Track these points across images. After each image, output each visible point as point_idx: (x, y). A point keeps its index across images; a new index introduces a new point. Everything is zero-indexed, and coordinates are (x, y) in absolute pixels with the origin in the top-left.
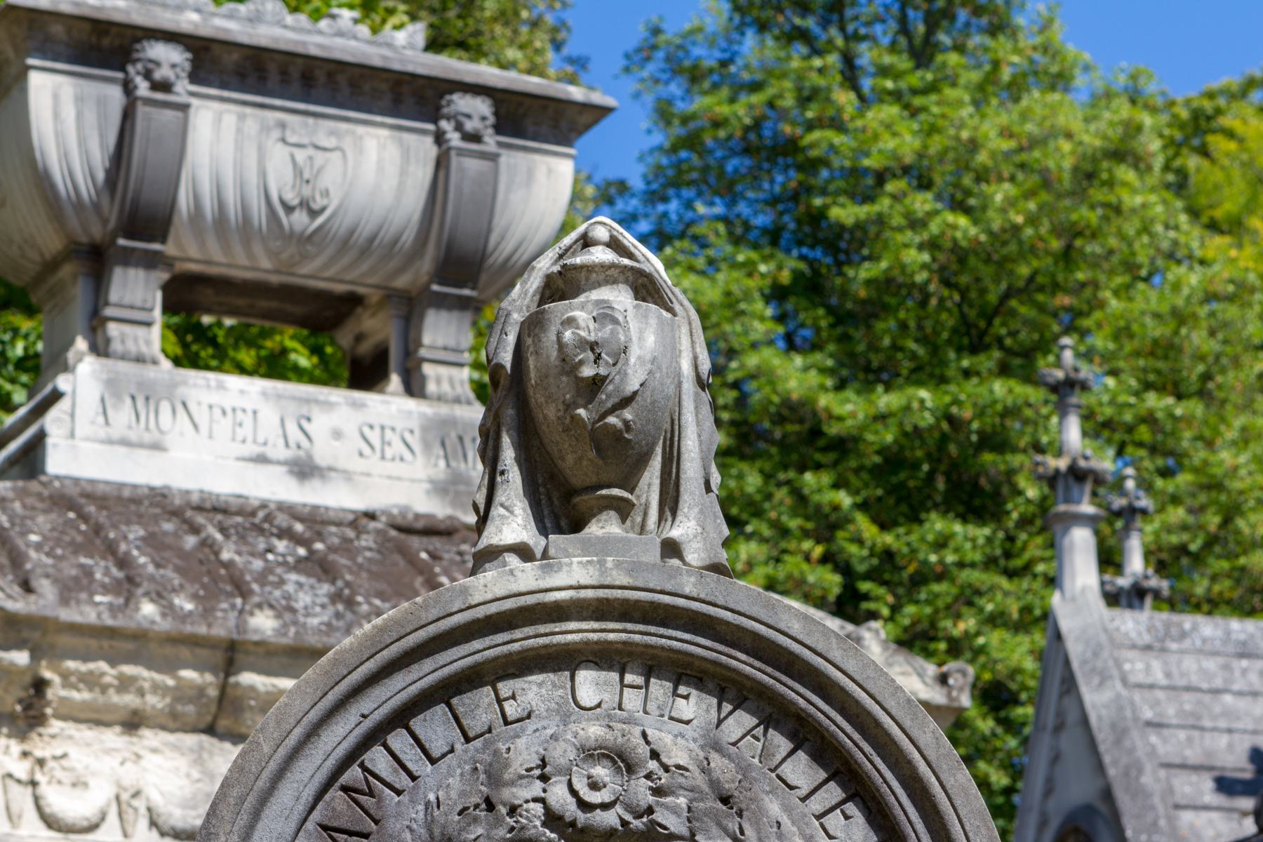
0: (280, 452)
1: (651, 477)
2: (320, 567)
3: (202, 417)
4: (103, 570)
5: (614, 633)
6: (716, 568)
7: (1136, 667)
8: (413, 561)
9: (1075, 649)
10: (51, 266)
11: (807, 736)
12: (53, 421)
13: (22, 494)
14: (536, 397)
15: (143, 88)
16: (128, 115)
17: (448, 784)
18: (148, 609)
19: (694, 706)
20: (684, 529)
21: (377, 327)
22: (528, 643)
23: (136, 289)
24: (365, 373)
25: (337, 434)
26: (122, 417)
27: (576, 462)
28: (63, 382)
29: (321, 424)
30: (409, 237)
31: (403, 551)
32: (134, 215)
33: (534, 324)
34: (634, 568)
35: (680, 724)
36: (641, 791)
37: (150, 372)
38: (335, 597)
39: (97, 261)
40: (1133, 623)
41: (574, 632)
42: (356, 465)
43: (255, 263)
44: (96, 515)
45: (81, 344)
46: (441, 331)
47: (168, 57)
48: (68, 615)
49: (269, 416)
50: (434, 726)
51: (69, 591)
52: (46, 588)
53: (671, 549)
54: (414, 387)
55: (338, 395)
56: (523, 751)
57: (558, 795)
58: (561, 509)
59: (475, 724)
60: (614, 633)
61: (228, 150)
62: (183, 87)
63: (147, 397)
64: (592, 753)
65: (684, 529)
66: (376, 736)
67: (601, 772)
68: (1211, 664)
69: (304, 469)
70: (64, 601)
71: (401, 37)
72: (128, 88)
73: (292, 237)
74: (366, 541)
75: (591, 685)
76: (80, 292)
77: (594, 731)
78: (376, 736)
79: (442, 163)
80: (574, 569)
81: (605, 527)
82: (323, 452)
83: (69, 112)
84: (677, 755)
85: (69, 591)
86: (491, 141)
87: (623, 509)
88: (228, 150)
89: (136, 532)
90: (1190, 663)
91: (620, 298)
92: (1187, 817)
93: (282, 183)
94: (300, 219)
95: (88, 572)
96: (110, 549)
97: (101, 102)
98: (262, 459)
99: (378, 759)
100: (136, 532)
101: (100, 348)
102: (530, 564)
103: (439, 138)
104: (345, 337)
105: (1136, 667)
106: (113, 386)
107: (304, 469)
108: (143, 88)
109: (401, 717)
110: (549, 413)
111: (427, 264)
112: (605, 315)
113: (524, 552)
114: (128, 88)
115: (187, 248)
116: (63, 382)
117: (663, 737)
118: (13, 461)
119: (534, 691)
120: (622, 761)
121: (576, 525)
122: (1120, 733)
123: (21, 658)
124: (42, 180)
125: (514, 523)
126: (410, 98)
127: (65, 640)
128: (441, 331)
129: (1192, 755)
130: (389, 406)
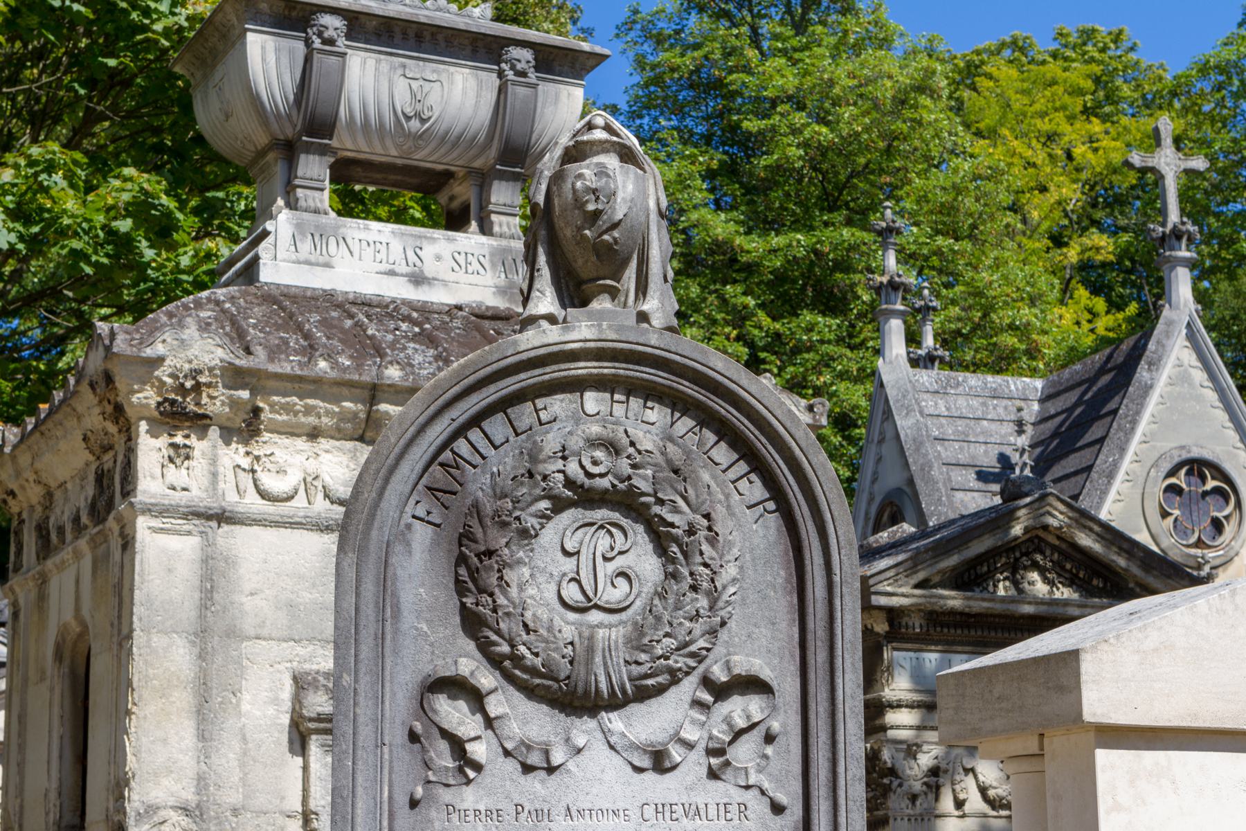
0: (403, 269)
1: (631, 273)
2: (429, 339)
3: (355, 247)
4: (294, 341)
5: (607, 369)
6: (670, 329)
7: (929, 404)
9: (891, 392)
10: (262, 153)
11: (726, 432)
12: (264, 249)
13: (244, 294)
14: (559, 223)
15: (317, 43)
16: (308, 60)
17: (505, 462)
18: (323, 364)
19: (657, 414)
20: (650, 305)
21: (463, 191)
22: (553, 375)
23: (314, 168)
24: (455, 220)
25: (438, 258)
26: (306, 246)
27: (584, 264)
28: (269, 225)
29: (428, 251)
30: (482, 136)
32: (312, 122)
33: (558, 178)
34: (620, 329)
35: (646, 425)
36: (624, 466)
37: (323, 219)
38: (437, 358)
39: (290, 150)
40: (926, 377)
41: (582, 368)
42: (451, 277)
43: (388, 152)
44: (290, 306)
45: (280, 202)
46: (502, 194)
47: (332, 23)
48: (273, 368)
49: (397, 246)
50: (497, 427)
52: (260, 352)
53: (643, 317)
54: (486, 229)
55: (438, 234)
56: (551, 441)
57: (573, 468)
58: (574, 292)
59: (521, 425)
60: (607, 369)
61: (370, 82)
62: (342, 42)
63: (321, 235)
64: (593, 443)
65: (650, 305)
66: (461, 432)
67: (599, 454)
68: (975, 403)
69: (418, 279)
70: (271, 359)
71: (477, 12)
73: (409, 135)
74: (457, 323)
75: (593, 401)
76: (279, 169)
77: (595, 429)
78: (461, 432)
79: (502, 90)
80: (583, 329)
81: (602, 304)
82: (430, 269)
84: (646, 444)
86: (532, 76)
87: (613, 293)
88: (370, 82)
89: (315, 317)
90: (961, 402)
91: (611, 161)
93: (403, 100)
94: (415, 125)
95: (286, 342)
96: (299, 328)
97: (291, 52)
98: (392, 273)
99: (462, 446)
100: (315, 317)
101: (292, 205)
102: (555, 326)
103: (501, 74)
104: (443, 198)
105: (929, 404)
106: (300, 227)
107: (418, 279)
108: (317, 43)
109: (476, 421)
110: (567, 233)
111: (493, 153)
112: (602, 172)
113: (552, 319)
114: (308, 43)
115: (345, 143)
116: (269, 225)
117: (638, 433)
118: (239, 274)
119: (558, 405)
120: (612, 447)
121: (584, 303)
122: (919, 444)
123: (245, 394)
124: (255, 99)
125: (545, 302)
126: (481, 49)
127: (271, 384)
128: (502, 194)
129: (963, 458)
130: (470, 241)
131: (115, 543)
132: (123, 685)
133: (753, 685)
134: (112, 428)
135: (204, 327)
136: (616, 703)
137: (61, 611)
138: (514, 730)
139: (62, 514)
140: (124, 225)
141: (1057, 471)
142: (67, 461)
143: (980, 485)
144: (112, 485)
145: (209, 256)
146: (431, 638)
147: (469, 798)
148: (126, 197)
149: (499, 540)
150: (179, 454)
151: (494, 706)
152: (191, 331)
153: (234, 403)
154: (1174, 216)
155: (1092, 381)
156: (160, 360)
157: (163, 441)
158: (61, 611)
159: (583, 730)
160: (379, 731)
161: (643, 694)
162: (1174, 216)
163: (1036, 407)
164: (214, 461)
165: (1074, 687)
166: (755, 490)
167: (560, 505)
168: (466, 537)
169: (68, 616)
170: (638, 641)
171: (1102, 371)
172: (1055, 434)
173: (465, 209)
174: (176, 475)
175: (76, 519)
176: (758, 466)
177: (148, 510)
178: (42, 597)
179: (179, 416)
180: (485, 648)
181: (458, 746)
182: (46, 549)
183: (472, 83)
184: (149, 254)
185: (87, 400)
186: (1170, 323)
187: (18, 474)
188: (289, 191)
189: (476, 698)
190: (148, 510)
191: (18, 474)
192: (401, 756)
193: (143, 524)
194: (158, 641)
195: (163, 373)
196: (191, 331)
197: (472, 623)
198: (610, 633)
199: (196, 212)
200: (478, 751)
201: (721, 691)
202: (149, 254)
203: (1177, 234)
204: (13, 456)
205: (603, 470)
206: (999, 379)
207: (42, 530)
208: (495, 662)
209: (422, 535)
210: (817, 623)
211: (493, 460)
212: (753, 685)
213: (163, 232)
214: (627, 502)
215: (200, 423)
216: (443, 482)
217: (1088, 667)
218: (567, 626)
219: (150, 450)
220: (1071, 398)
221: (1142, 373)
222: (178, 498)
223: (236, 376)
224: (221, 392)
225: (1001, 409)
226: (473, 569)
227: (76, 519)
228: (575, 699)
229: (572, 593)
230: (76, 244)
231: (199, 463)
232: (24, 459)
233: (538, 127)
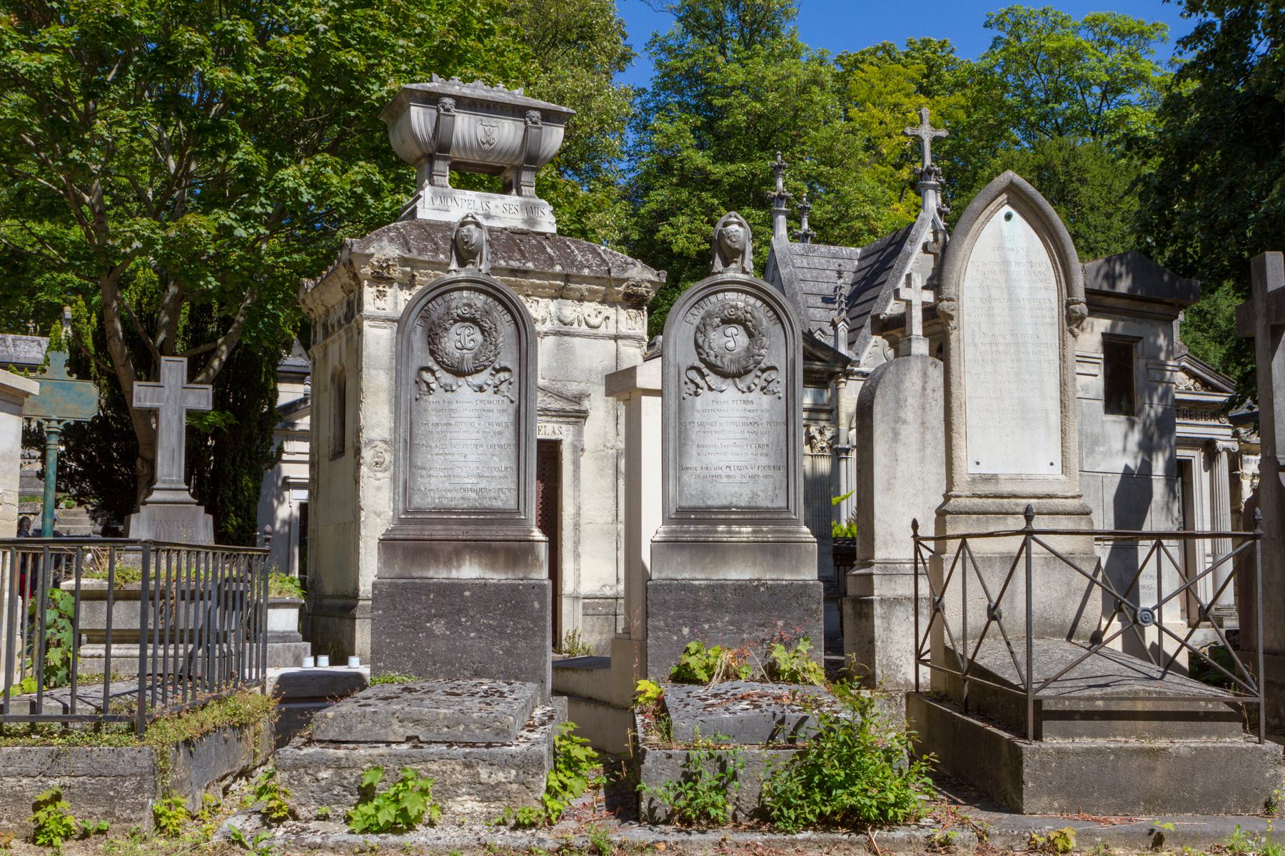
4: (430, 246)
5: (469, 285)
7: (798, 261)
8: (515, 242)
9: (778, 255)
10: (418, 159)
15: (442, 111)
16: (438, 118)
17: (441, 310)
18: (442, 256)
19: (482, 297)
21: (510, 175)
22: (454, 286)
23: (441, 166)
24: (506, 190)
26: (437, 202)
27: (465, 255)
28: (421, 193)
29: (492, 204)
30: (517, 151)
31: (512, 239)
32: (440, 146)
35: (480, 300)
37: (445, 190)
39: (431, 158)
40: (798, 247)
43: (475, 158)
44: (430, 229)
46: (526, 177)
47: (449, 102)
48: (420, 258)
49: (478, 202)
50: (439, 300)
51: (420, 252)
52: (414, 251)
54: (519, 193)
55: (497, 196)
56: (453, 305)
58: (462, 263)
60: (469, 285)
61: (466, 127)
62: (453, 109)
63: (444, 197)
66: (430, 302)
68: (823, 261)
71: (517, 92)
72: (438, 110)
73: (484, 151)
74: (504, 237)
75: (465, 293)
76: (426, 167)
78: (430, 302)
79: (526, 130)
80: (463, 274)
81: (470, 266)
83: (422, 118)
85: (420, 252)
86: (540, 124)
88: (466, 127)
89: (440, 235)
90: (816, 260)
91: (472, 227)
92: (811, 310)
93: (481, 136)
94: (487, 146)
96: (433, 240)
97: (431, 114)
100: (440, 235)
101: (432, 183)
102: (456, 272)
103: (526, 123)
104: (502, 178)
105: (798, 261)
106: (435, 194)
108: (442, 111)
109: (434, 299)
111: (522, 158)
112: (469, 230)
114: (438, 110)
115: (454, 154)
116: (421, 193)
119: (456, 294)
120: (470, 306)
122: (791, 283)
123: (408, 269)
124: (414, 136)
125: (454, 266)
126: (517, 111)
128: (526, 177)
129: (815, 290)
130: (512, 199)
131: (355, 331)
132: (359, 390)
133: (506, 369)
134: (353, 283)
135: (391, 240)
136: (470, 374)
137: (333, 361)
138: (443, 381)
139: (333, 319)
140: (359, 190)
141: (863, 298)
142: (335, 296)
143: (824, 305)
144: (354, 306)
145: (398, 202)
146: (421, 356)
147: (431, 398)
148: (360, 177)
149: (439, 331)
150: (381, 294)
152: (385, 242)
153: (404, 273)
154: (928, 162)
155: (884, 250)
156: (372, 255)
157: (374, 289)
158: (333, 361)
159: (461, 381)
160: (407, 379)
161: (477, 372)
162: (928, 162)
163: (856, 263)
164: (396, 297)
165: (634, 378)
166: (508, 317)
167: (456, 322)
168: (431, 330)
169: (336, 363)
170: (475, 358)
171: (889, 245)
172: (864, 278)
173: (511, 183)
174: (380, 303)
175: (339, 321)
176: (510, 311)
177: (368, 318)
178: (325, 355)
179: (381, 278)
180: (435, 359)
181: (428, 384)
182: (327, 334)
183: (512, 127)
184: (371, 201)
185: (342, 270)
186: (923, 220)
187: (314, 301)
188: (431, 177)
189: (433, 372)
190: (368, 318)
191: (314, 301)
192: (414, 387)
193: (366, 323)
194: (373, 372)
195: (374, 261)
196: (385, 242)
197: (432, 353)
198: (468, 355)
199: (393, 180)
200: (433, 386)
201: (498, 371)
202: (371, 201)
203: (929, 172)
204: (312, 294)
205: (466, 312)
206: (837, 248)
207: (325, 326)
208: (438, 363)
209: (419, 329)
211: (438, 309)
212: (506, 369)
213: (377, 192)
214: (474, 321)
215: (389, 281)
216: (425, 315)
217: (639, 371)
218: (457, 354)
219: (369, 293)
220: (874, 258)
221: (907, 247)
222: (381, 313)
223: (404, 261)
224: (398, 268)
225: (834, 265)
226: (433, 338)
227: (339, 321)
228: (459, 373)
229: (459, 345)
230: (338, 200)
231: (389, 298)
232: (317, 295)
233: (543, 146)
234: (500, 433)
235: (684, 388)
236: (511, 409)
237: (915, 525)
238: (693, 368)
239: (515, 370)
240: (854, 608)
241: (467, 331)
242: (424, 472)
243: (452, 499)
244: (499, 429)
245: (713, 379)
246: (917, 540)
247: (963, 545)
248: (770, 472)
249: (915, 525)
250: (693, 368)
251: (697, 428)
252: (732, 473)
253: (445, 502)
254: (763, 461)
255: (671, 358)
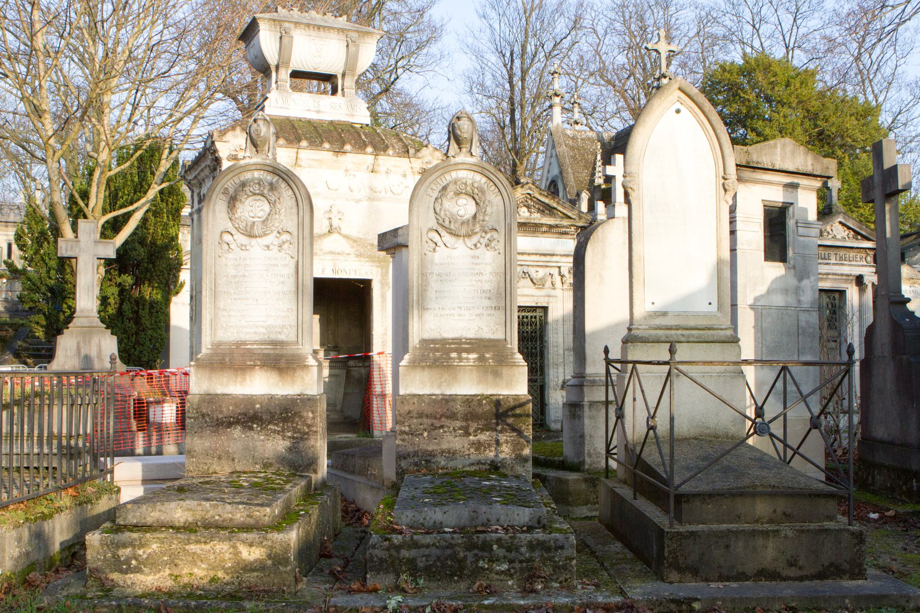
12: (266, 103)
28: (268, 95)
98: (309, 110)
147: (230, 256)
151: (235, 237)
159: (254, 241)
166: (290, 192)
210: (300, 220)
229: (252, 215)
234: (283, 283)
235: (426, 246)
236: (292, 264)
237: (606, 351)
238: (431, 230)
239: (295, 233)
240: (570, 411)
241: (258, 204)
242: (225, 313)
243: (247, 334)
244: (282, 279)
245: (447, 238)
246: (609, 362)
247: (634, 368)
248: (493, 312)
249: (606, 351)
250: (431, 230)
251: (435, 278)
252: (463, 312)
253: (242, 336)
254: (487, 303)
255: (415, 223)
